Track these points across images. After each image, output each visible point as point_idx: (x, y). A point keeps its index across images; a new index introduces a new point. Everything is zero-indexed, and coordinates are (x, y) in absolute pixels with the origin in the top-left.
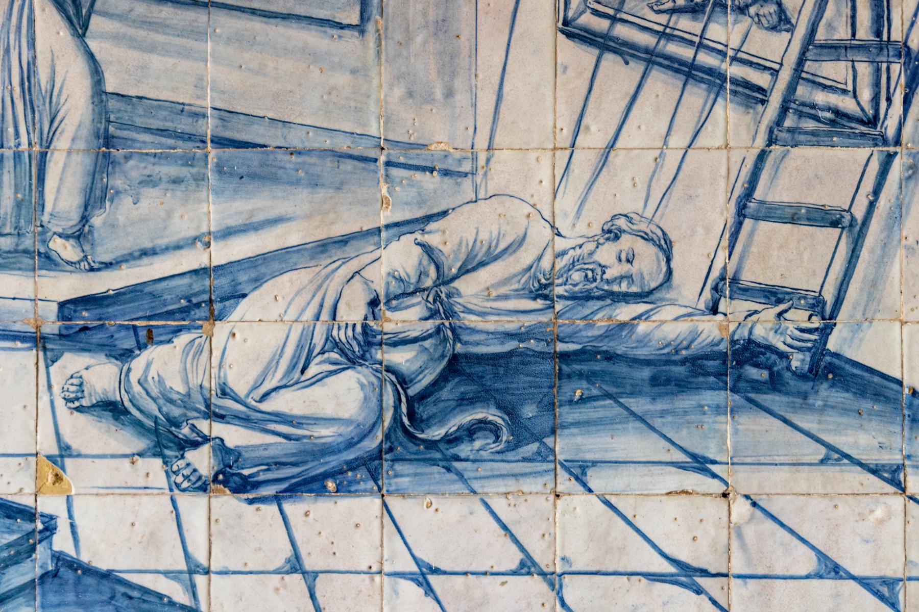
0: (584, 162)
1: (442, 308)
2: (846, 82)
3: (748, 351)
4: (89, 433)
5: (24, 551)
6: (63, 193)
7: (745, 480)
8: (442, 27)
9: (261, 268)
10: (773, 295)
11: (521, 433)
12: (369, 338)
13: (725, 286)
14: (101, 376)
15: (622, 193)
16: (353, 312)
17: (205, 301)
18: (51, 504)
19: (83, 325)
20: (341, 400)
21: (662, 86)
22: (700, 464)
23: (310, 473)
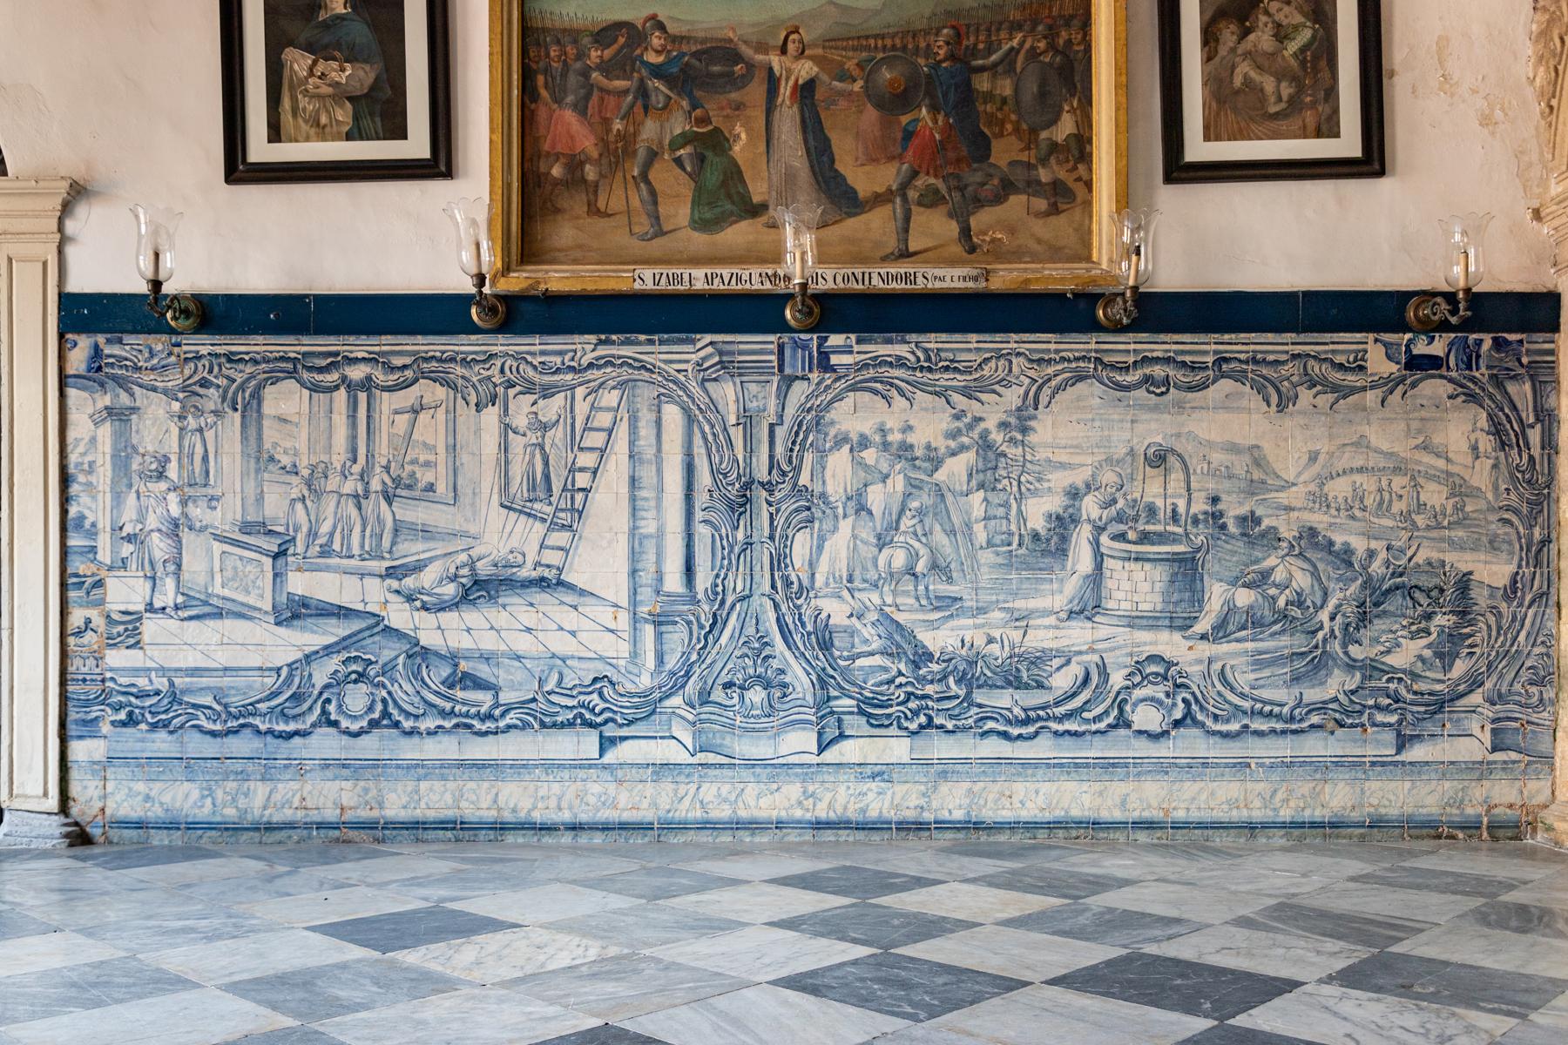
0: (505, 535)
1: (473, 569)
2: (565, 517)
3: (543, 579)
4: (392, 597)
5: (378, 624)
6: (386, 543)
7: (541, 608)
8: (473, 505)
9: (431, 560)
10: (548, 566)
11: (491, 598)
12: (456, 576)
13: (538, 564)
14: (395, 584)
15: (514, 542)
16: (452, 570)
17: (418, 567)
18: (383, 613)
19: (391, 573)
20: (450, 590)
21: (523, 518)
22: (532, 605)
23: (442, 608)
